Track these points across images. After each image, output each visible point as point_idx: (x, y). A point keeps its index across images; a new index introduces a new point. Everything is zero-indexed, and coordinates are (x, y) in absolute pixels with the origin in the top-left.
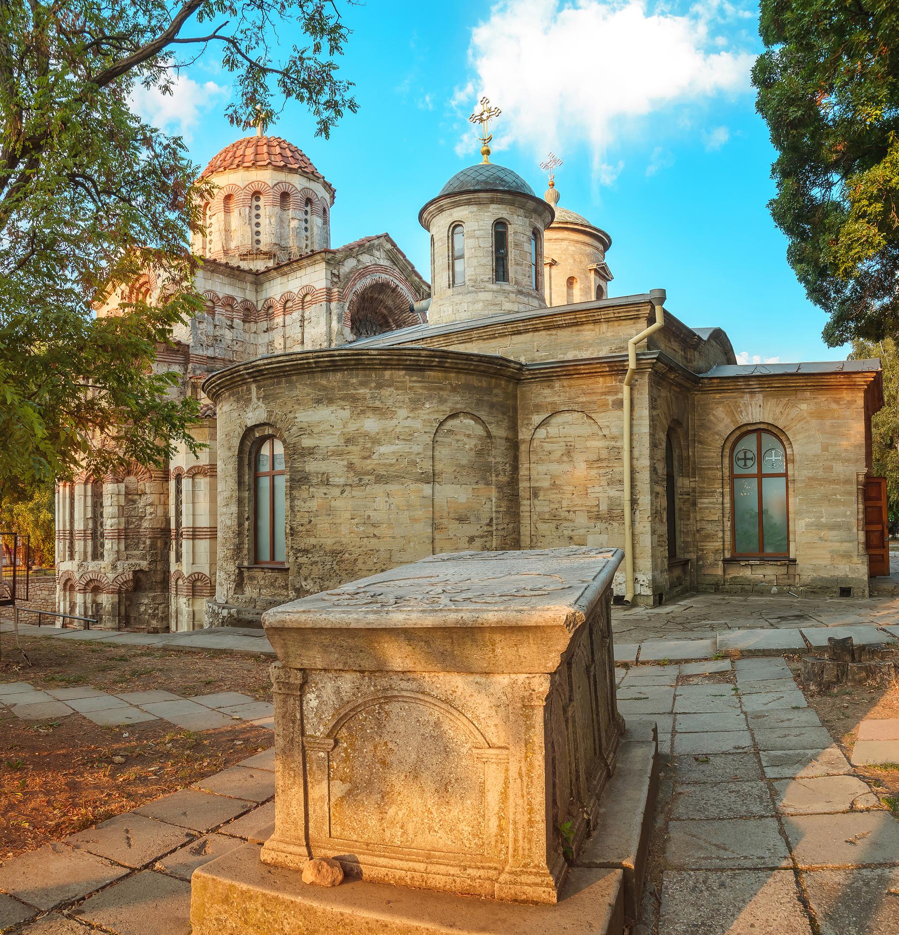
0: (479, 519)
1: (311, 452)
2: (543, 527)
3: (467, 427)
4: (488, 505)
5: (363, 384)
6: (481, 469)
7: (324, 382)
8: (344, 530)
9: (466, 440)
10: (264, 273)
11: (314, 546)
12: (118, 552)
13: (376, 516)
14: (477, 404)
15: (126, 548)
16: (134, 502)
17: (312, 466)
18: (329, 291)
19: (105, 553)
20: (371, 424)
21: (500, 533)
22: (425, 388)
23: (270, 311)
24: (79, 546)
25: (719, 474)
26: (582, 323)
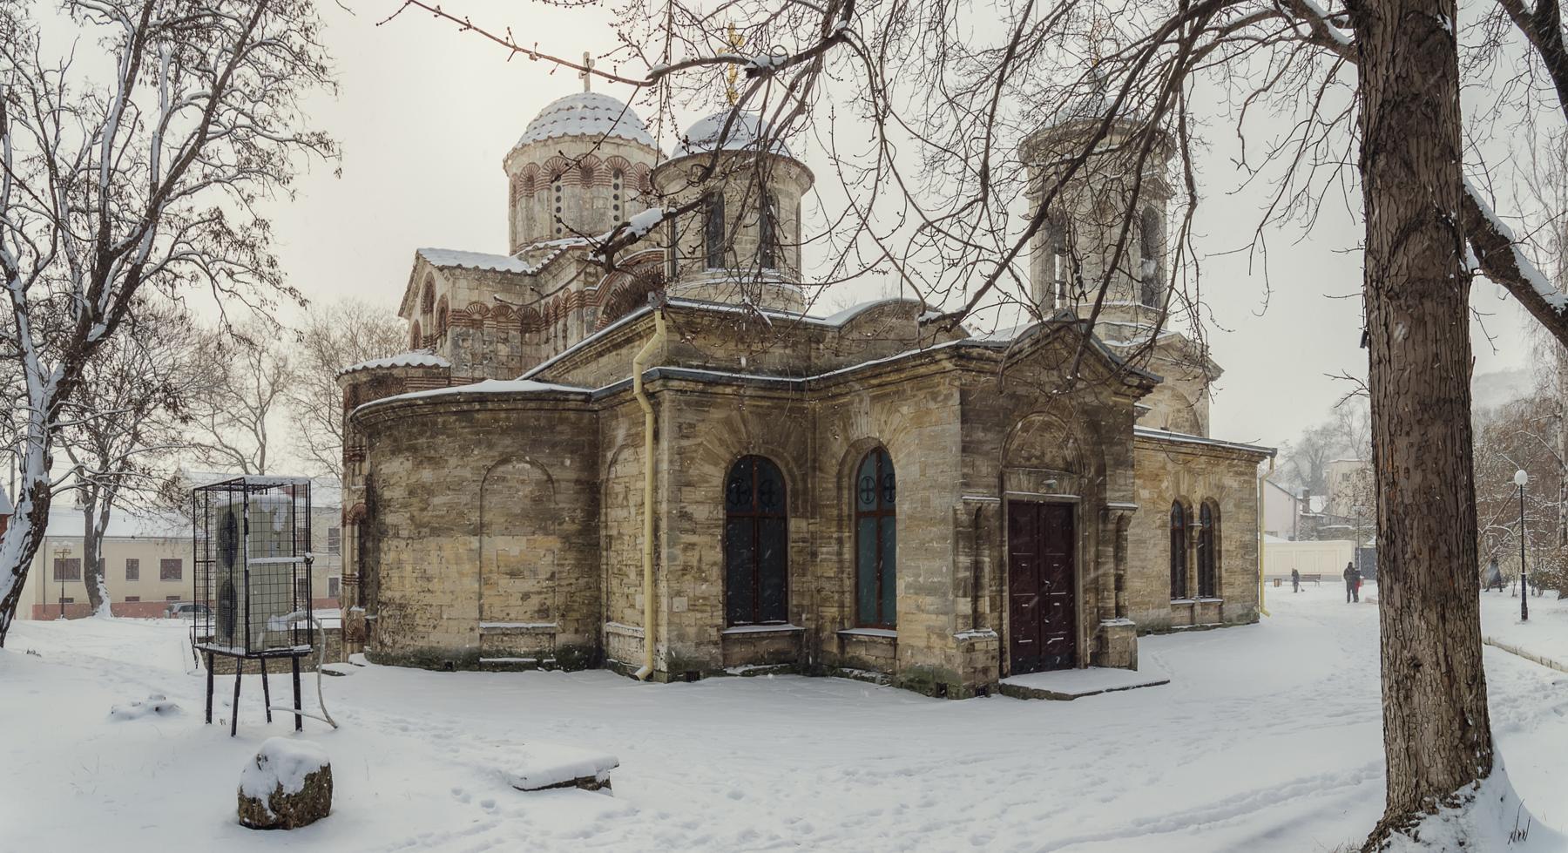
3: (520, 471)
4: (549, 558)
5: (421, 434)
6: (539, 516)
20: (427, 475)
25: (835, 512)
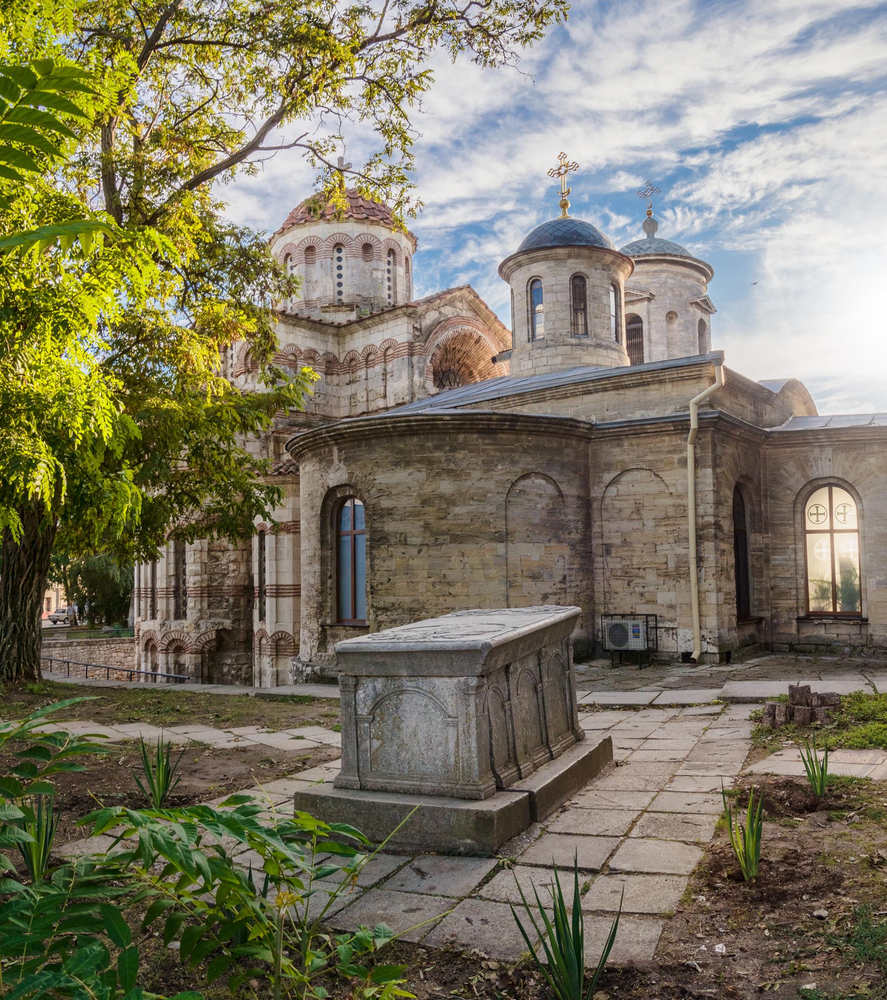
0: (551, 576)
1: (390, 512)
2: (616, 584)
3: (539, 487)
4: (561, 563)
5: (438, 448)
6: (554, 528)
7: (402, 446)
8: (421, 588)
9: (537, 499)
10: (345, 326)
11: (393, 604)
12: (200, 610)
13: (452, 576)
14: (548, 464)
15: (209, 606)
16: (217, 559)
17: (390, 526)
18: (411, 346)
19: (188, 612)
20: (446, 486)
21: (574, 590)
22: (496, 450)
23: (353, 363)
24: (161, 604)
26: (648, 384)
